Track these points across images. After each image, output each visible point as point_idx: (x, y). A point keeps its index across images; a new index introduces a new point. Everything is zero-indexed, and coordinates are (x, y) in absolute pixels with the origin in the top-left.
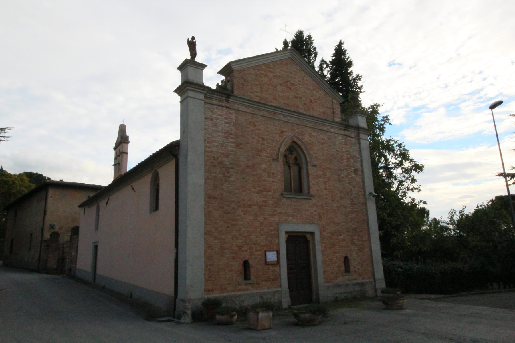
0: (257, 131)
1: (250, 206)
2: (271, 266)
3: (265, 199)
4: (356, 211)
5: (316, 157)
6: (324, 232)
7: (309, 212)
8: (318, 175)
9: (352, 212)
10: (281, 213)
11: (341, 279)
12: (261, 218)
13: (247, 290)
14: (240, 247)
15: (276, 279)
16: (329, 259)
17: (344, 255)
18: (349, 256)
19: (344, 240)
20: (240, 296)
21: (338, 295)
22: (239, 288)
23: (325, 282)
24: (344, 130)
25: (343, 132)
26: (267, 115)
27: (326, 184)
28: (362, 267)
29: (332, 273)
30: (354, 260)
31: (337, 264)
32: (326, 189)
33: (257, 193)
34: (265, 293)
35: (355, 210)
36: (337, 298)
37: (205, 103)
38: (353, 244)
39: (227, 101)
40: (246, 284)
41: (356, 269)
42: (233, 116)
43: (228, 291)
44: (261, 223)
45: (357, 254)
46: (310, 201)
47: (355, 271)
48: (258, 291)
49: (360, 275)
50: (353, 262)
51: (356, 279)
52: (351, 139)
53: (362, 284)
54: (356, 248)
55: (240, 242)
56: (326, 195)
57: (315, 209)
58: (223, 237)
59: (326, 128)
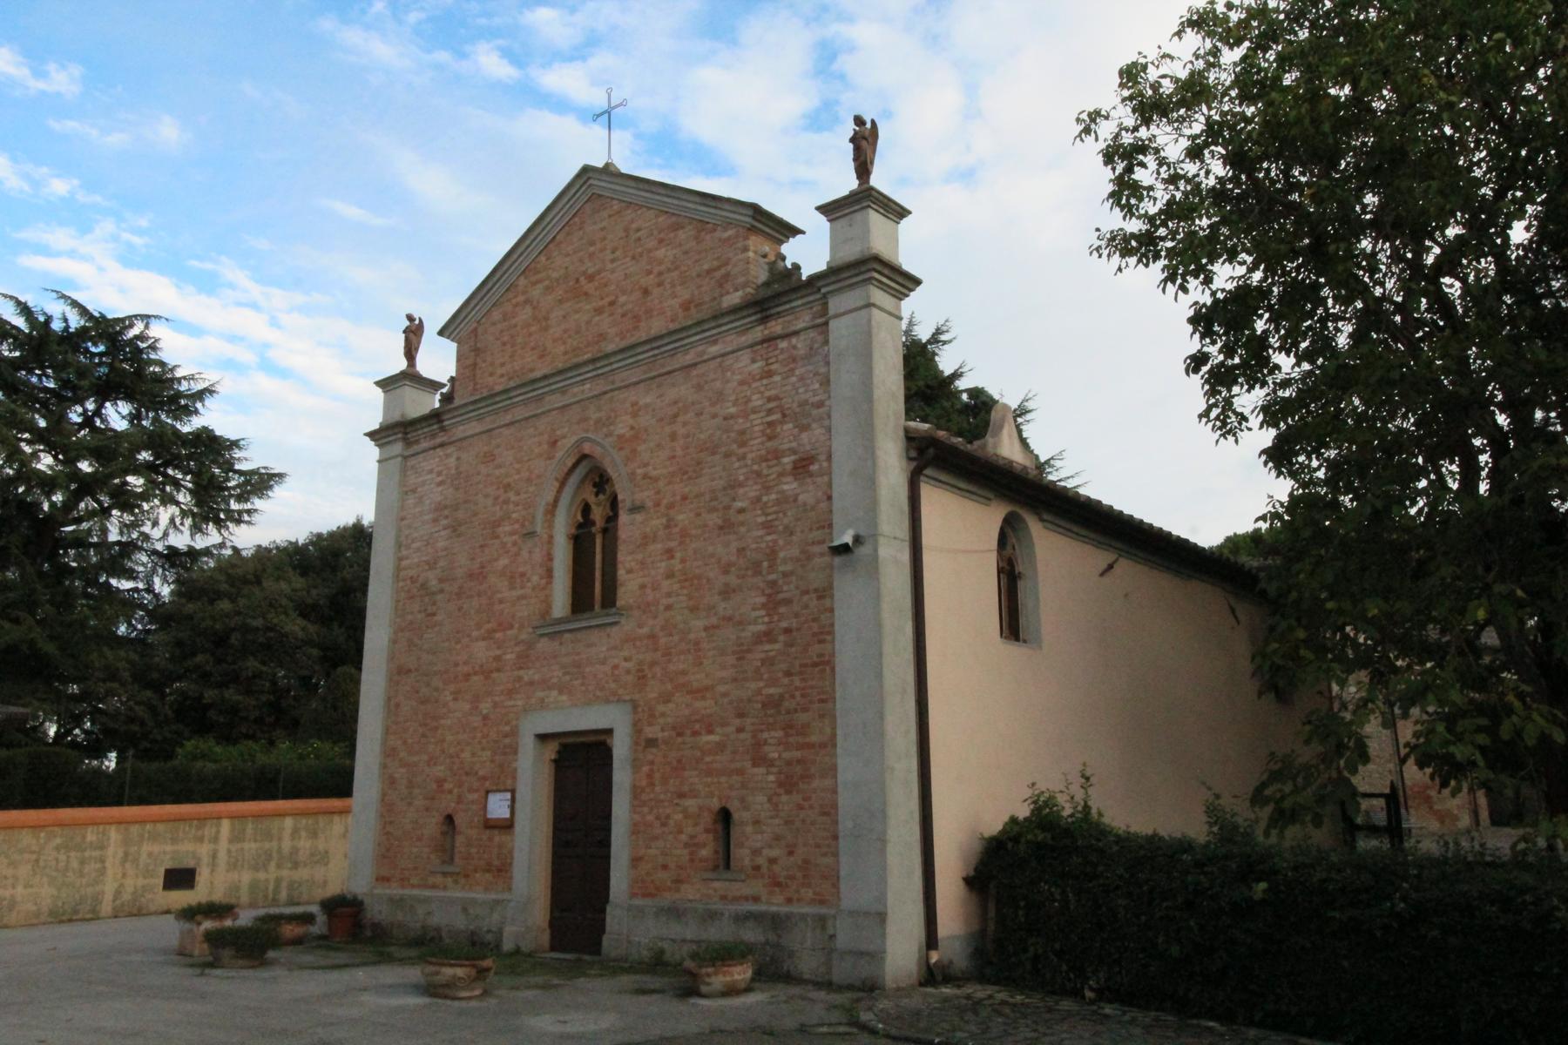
0: (497, 472)
1: (467, 676)
2: (496, 832)
3: (498, 652)
4: (787, 631)
5: (645, 476)
6: (650, 724)
7: (607, 668)
8: (645, 537)
9: (768, 636)
10: (531, 683)
11: (691, 892)
12: (485, 707)
13: (445, 888)
14: (440, 782)
15: (501, 870)
16: (657, 818)
17: (715, 804)
18: (734, 806)
19: (720, 747)
20: (426, 900)
21: (666, 945)
22: (431, 880)
23: (633, 895)
24: (764, 320)
25: (758, 333)
26: (520, 413)
27: (672, 557)
28: (791, 853)
29: (665, 867)
30: (757, 822)
31: (683, 837)
32: (670, 575)
33: (484, 639)
34: (474, 901)
35: (784, 624)
36: (662, 952)
37: (405, 458)
38: (759, 760)
39: (443, 429)
40: (445, 874)
41: (761, 861)
42: (452, 461)
43: (413, 886)
44: (485, 718)
45: (770, 800)
46: (615, 629)
47: (757, 868)
48: (459, 895)
49: (778, 884)
50: (749, 829)
51: (756, 899)
52: (794, 340)
53: (776, 922)
54: (771, 778)
55: (439, 770)
56: (669, 595)
57: (626, 653)
58: (415, 759)
59: (690, 358)
